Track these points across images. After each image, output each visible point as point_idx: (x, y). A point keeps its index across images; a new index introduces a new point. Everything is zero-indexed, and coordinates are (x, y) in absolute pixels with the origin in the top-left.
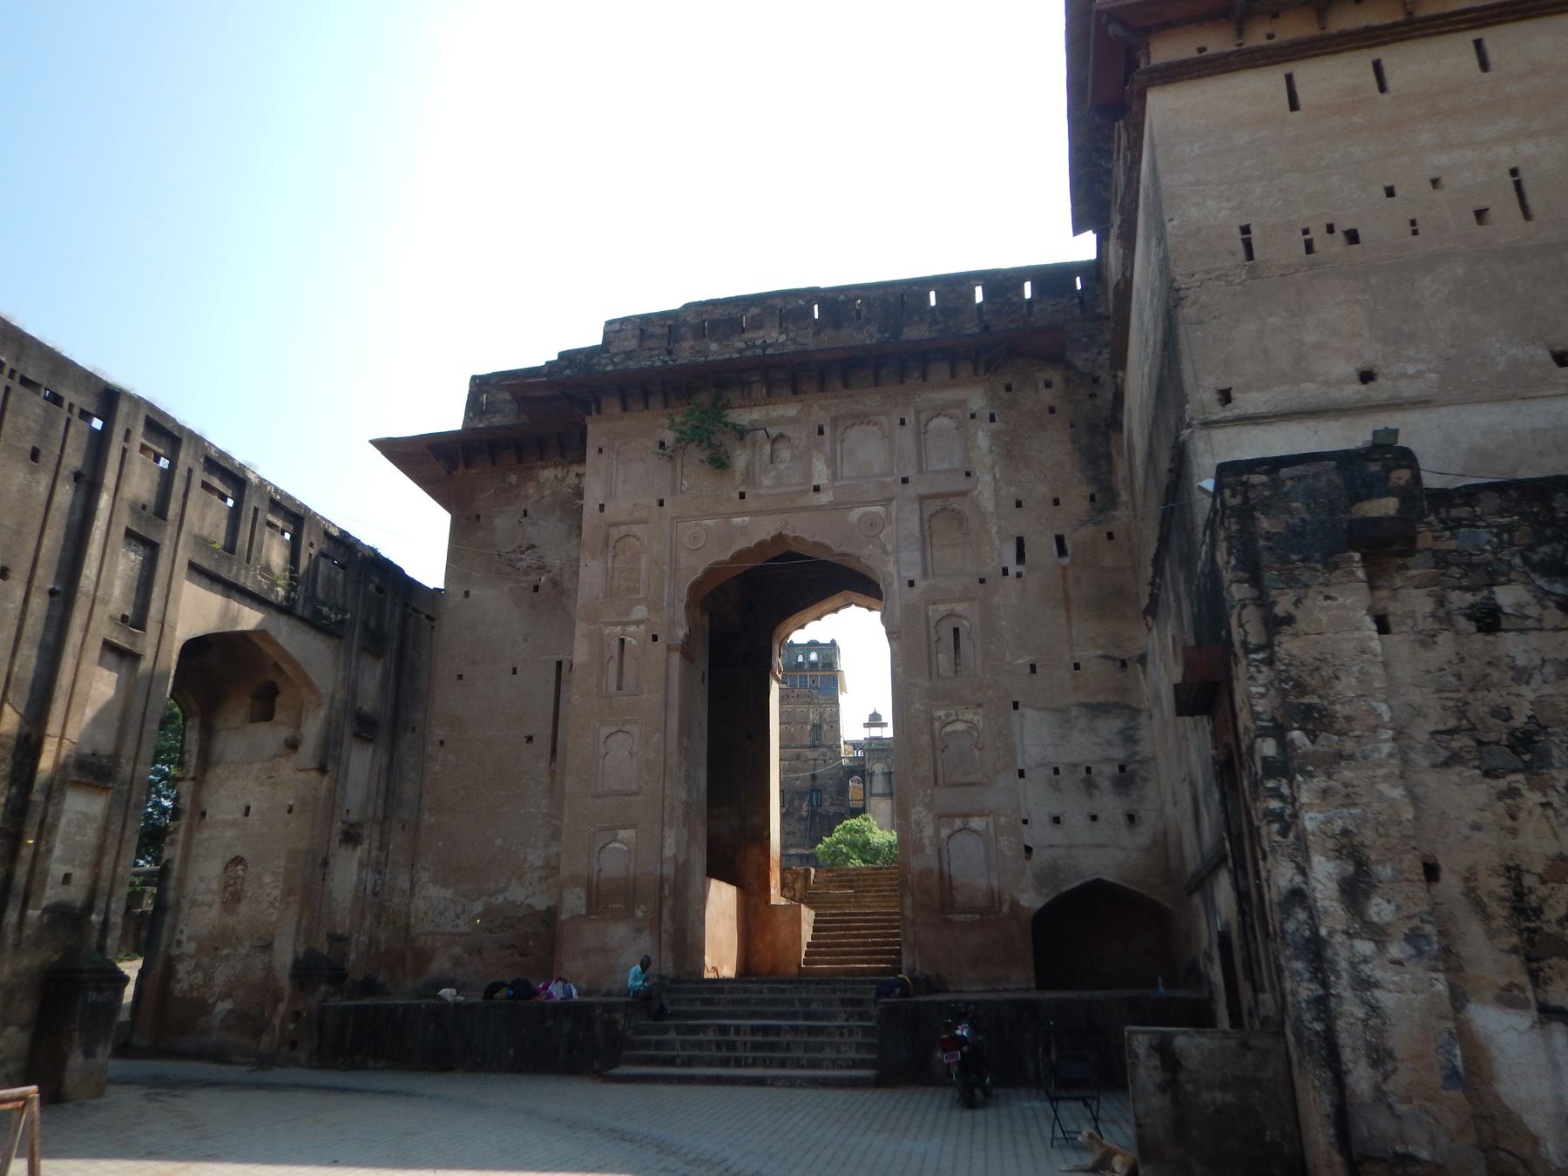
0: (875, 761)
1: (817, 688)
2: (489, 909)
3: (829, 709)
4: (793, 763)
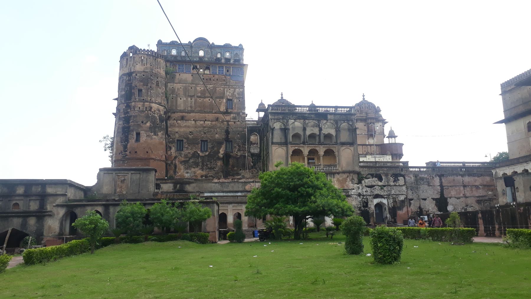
0: (275, 121)
1: (230, 75)
4: (214, 123)
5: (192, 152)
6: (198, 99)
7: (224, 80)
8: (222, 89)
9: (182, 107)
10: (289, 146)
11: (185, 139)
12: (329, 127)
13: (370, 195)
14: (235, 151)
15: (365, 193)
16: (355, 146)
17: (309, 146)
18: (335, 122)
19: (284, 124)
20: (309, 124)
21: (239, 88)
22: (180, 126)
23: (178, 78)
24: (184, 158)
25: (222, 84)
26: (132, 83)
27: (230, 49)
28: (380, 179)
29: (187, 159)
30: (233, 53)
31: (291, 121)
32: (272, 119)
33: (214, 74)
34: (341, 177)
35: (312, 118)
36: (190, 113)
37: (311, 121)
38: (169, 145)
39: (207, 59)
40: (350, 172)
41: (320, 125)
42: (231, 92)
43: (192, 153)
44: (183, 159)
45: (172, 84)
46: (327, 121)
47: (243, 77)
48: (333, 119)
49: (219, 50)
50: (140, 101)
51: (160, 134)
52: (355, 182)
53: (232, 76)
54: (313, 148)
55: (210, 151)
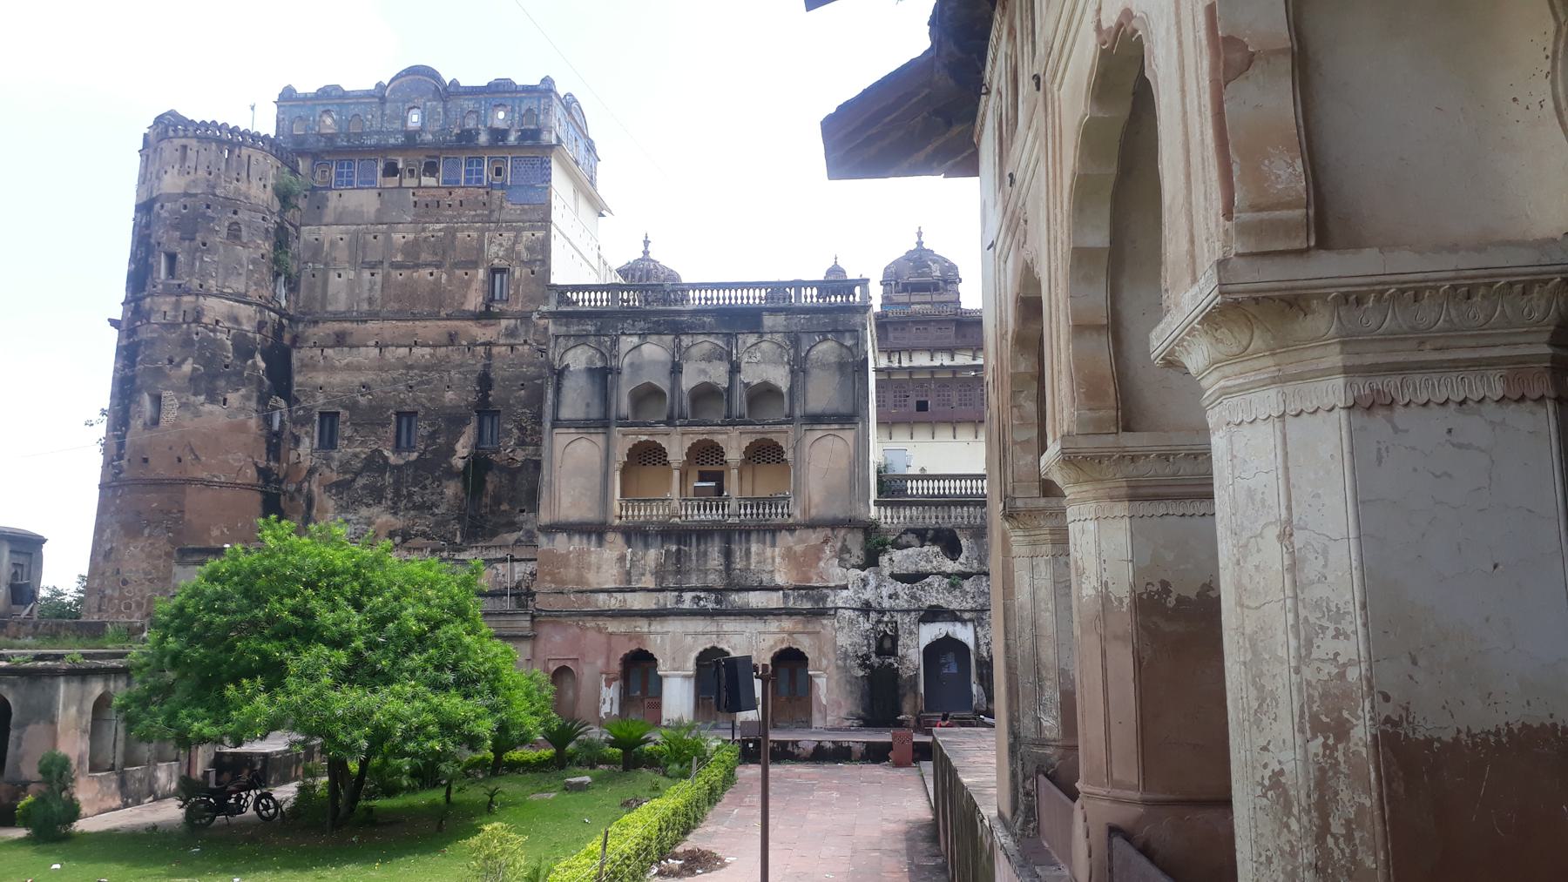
0: (571, 343)
1: (503, 186)
3: (529, 234)
4: (442, 351)
5: (363, 451)
6: (395, 273)
7: (484, 204)
8: (474, 235)
9: (340, 304)
10: (617, 431)
11: (346, 408)
12: (763, 361)
13: (908, 611)
14: (509, 447)
15: (886, 604)
16: (860, 426)
17: (689, 429)
18: (791, 342)
19: (602, 354)
20: (694, 351)
21: (533, 228)
22: (331, 368)
23: (335, 208)
24: (338, 473)
25: (477, 219)
26: (149, 236)
27: (507, 95)
28: (953, 550)
29: (347, 476)
30: (517, 108)
31: (627, 342)
32: (557, 337)
33: (450, 185)
34: (801, 541)
35: (704, 328)
36: (366, 321)
37: (701, 338)
38: (294, 431)
39: (431, 137)
40: (834, 524)
41: (734, 351)
42: (504, 243)
43: (363, 456)
44: (335, 477)
45: (313, 227)
46: (761, 337)
47: (547, 188)
48: (781, 329)
49: (469, 104)
50: (167, 291)
51: (234, 398)
52: (854, 561)
53: (510, 187)
54: (705, 436)
55: (422, 447)
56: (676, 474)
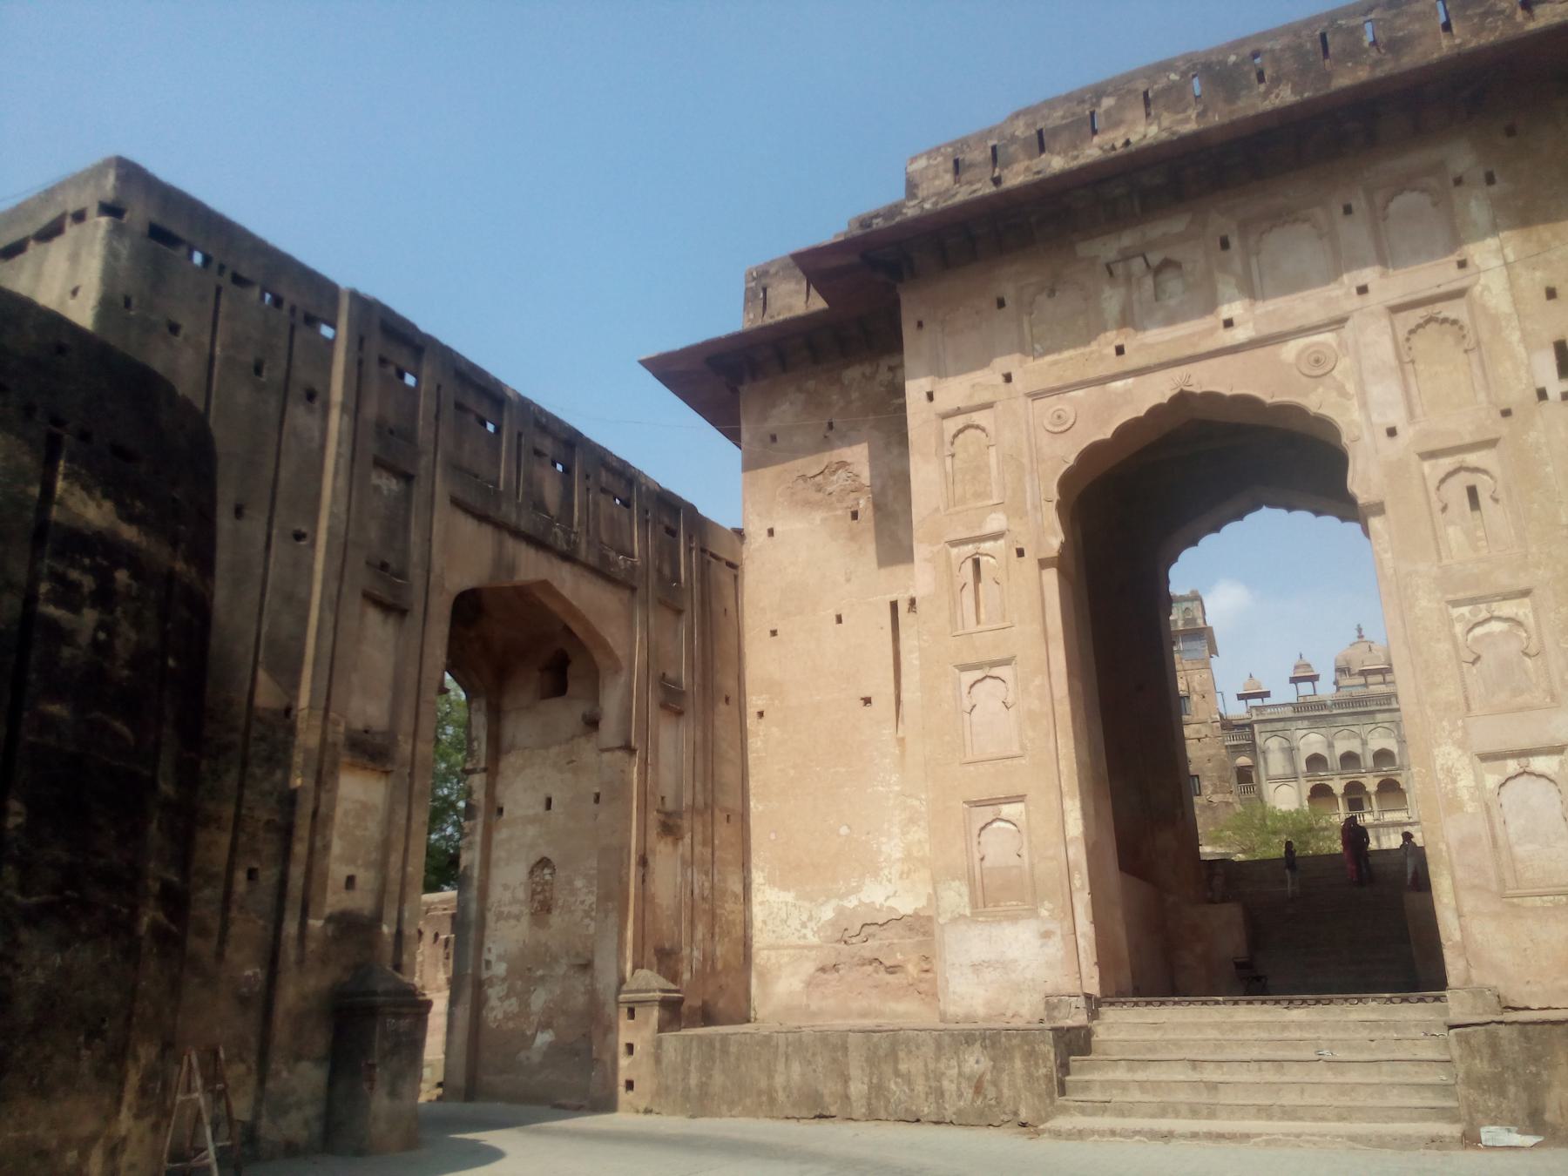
2: (840, 912)
56: (1340, 800)
